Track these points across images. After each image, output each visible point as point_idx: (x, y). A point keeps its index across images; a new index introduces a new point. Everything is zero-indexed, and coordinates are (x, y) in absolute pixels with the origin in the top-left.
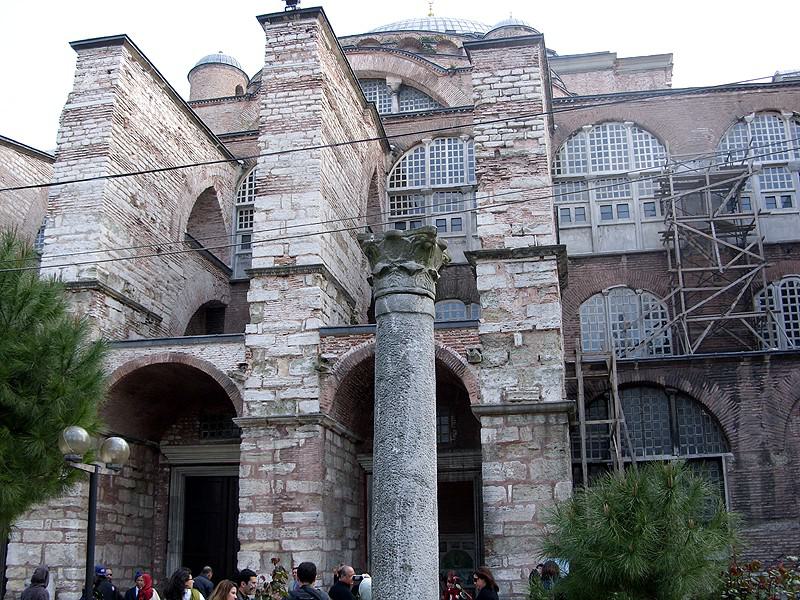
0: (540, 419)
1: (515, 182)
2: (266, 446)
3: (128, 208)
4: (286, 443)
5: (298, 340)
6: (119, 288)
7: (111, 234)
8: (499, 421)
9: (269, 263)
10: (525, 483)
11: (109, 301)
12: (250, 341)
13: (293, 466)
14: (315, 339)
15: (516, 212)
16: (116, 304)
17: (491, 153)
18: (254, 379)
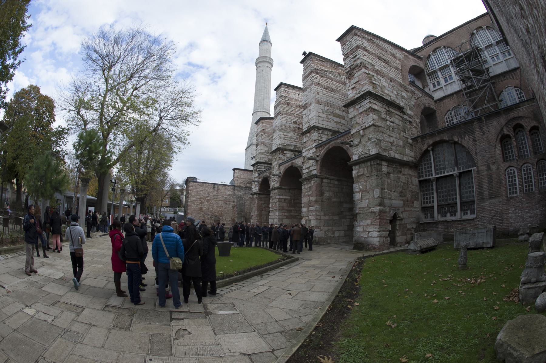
0: (369, 164)
1: (356, 75)
2: (306, 187)
3: (293, 125)
4: (310, 185)
5: (311, 151)
6: (292, 148)
7: (285, 134)
8: (357, 167)
9: (306, 129)
10: (365, 191)
11: (285, 152)
12: (304, 155)
13: (311, 192)
14: (314, 150)
15: (358, 86)
16: (289, 152)
17: (349, 69)
18: (304, 168)
